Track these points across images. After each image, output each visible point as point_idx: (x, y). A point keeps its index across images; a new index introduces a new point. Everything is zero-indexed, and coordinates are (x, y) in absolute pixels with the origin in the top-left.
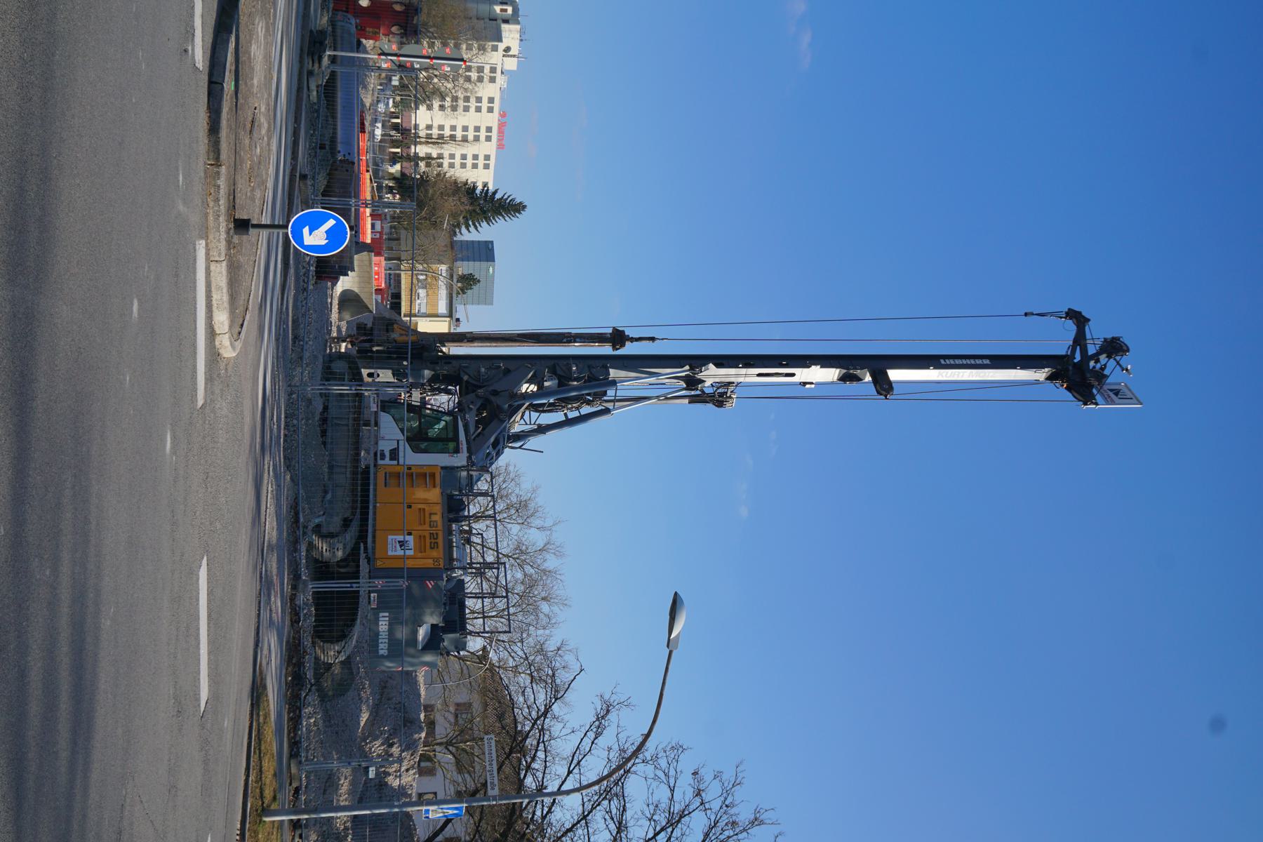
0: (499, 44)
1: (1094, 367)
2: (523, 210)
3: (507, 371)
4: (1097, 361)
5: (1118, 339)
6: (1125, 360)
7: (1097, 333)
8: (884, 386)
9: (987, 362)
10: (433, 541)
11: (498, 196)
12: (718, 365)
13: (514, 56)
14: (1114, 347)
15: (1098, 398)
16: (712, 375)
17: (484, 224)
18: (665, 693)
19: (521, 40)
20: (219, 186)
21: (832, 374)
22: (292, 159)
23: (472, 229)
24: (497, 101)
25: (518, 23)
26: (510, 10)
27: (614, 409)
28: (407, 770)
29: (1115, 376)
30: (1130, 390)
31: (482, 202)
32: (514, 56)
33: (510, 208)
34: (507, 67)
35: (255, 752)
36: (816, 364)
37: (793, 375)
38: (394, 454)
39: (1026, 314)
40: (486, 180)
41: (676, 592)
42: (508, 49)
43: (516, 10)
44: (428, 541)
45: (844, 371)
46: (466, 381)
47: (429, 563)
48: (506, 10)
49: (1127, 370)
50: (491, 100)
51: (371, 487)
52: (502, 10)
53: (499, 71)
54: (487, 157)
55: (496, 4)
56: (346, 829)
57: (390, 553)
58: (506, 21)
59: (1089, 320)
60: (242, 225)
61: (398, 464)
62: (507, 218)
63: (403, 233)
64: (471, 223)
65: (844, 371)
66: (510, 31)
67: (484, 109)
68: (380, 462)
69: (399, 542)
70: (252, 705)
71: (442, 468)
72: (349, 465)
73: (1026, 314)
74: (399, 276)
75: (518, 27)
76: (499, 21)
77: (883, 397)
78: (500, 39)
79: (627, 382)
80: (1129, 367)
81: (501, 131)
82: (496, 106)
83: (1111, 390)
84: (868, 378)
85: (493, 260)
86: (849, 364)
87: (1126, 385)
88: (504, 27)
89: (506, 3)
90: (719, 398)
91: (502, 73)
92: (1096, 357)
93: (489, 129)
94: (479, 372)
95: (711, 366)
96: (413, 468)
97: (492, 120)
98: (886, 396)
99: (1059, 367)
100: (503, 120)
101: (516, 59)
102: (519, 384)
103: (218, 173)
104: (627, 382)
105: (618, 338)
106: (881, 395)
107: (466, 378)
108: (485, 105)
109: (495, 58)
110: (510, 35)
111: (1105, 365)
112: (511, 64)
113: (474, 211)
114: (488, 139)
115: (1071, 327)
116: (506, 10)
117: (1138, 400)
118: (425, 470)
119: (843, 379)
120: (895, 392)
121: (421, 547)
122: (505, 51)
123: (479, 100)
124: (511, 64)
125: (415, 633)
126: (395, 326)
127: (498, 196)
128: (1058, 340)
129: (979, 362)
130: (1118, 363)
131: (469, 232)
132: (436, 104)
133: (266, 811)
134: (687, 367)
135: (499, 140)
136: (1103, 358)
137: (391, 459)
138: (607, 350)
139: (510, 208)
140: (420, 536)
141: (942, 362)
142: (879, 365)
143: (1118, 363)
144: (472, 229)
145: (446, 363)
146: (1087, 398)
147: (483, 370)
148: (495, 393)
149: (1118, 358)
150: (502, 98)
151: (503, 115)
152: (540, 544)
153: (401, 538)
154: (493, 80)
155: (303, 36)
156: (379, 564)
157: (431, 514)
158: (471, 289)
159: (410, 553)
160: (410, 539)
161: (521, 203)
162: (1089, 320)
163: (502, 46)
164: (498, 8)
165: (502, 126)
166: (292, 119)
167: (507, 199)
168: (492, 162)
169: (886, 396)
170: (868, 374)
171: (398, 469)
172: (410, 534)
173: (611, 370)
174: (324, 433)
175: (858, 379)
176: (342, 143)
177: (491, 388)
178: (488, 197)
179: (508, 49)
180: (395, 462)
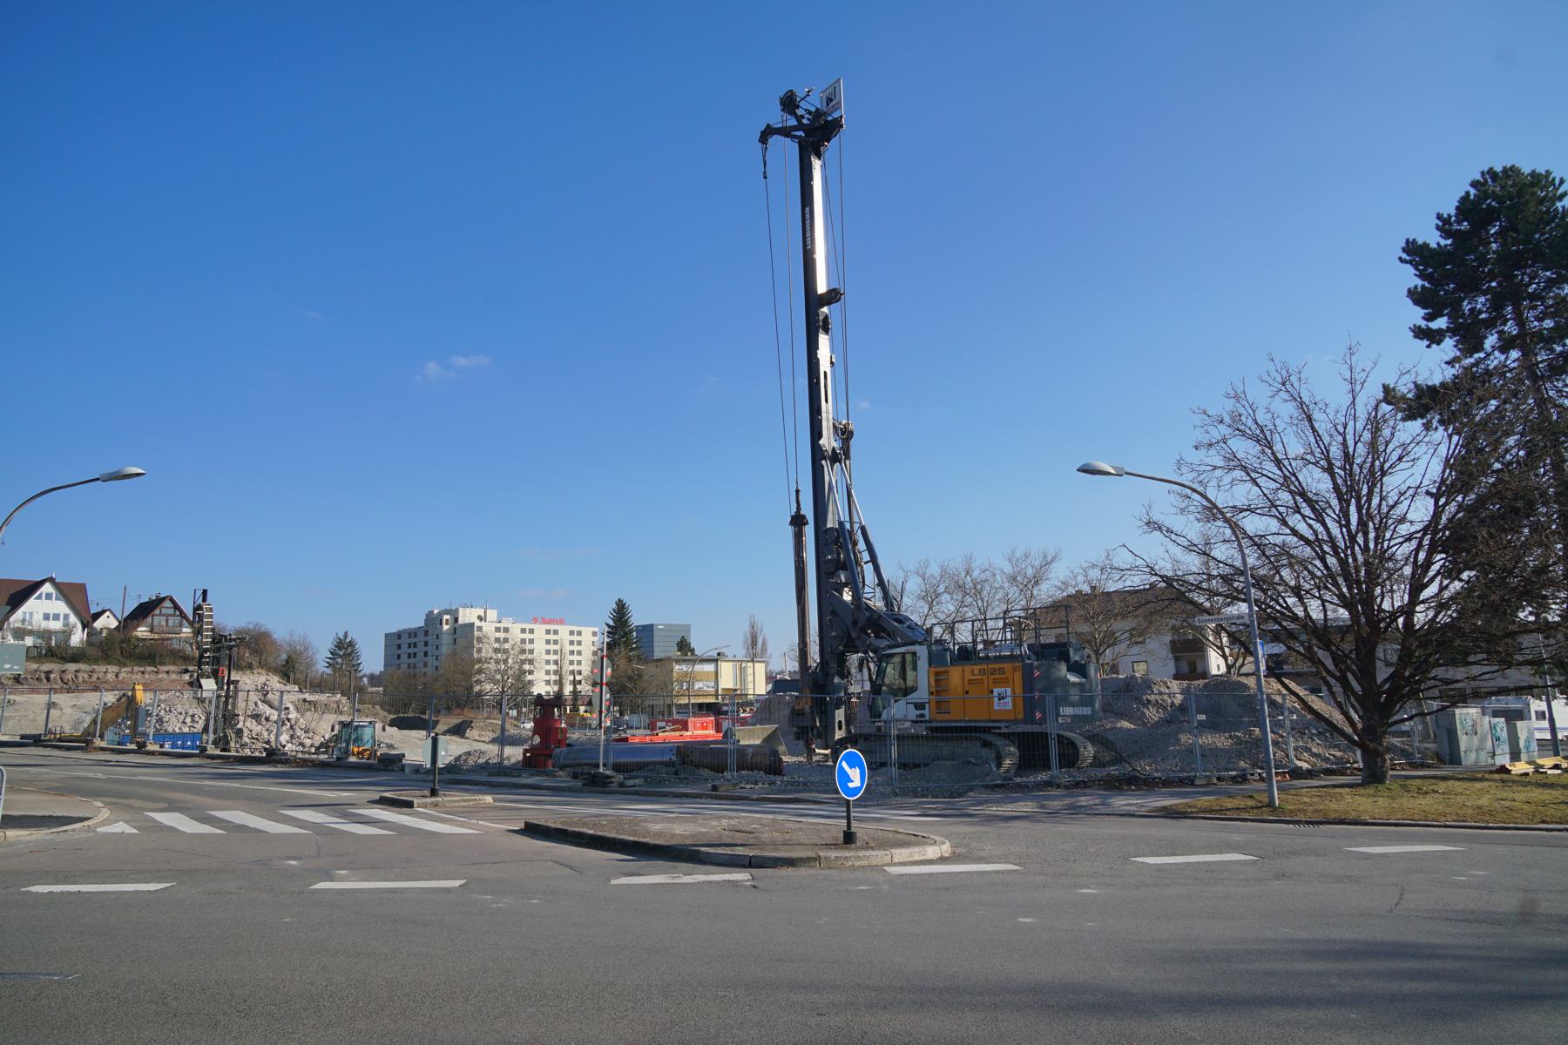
0: (476, 625)
1: (809, 119)
3: (834, 613)
4: (803, 117)
5: (781, 99)
6: (800, 94)
7: (777, 118)
8: (833, 296)
9: (807, 210)
10: (997, 672)
11: (611, 623)
12: (820, 436)
13: (485, 612)
14: (789, 103)
15: (836, 115)
16: (828, 441)
18: (1159, 477)
19: (472, 607)
20: (836, 857)
21: (823, 340)
22: (701, 798)
24: (524, 626)
25: (457, 609)
26: (446, 617)
27: (860, 523)
28: (1168, 688)
29: (814, 102)
30: (827, 89)
31: (617, 637)
32: (485, 612)
33: (621, 611)
34: (495, 619)
35: (1225, 814)
36: (817, 354)
37: (825, 373)
38: (920, 706)
39: (765, 178)
40: (591, 634)
41: (1078, 470)
42: (480, 618)
43: (447, 612)
44: (998, 676)
45: (821, 330)
46: (844, 647)
47: (1018, 676)
48: (447, 620)
49: (809, 92)
50: (523, 631)
51: (953, 724)
52: (447, 624)
54: (572, 633)
55: (442, 629)
56: (1231, 737)
57: (1010, 707)
58: (456, 620)
59: (768, 125)
60: (849, 838)
61: (929, 703)
62: (630, 615)
63: (647, 703)
65: (821, 330)
66: (464, 616)
67: (531, 636)
68: (927, 718)
69: (999, 700)
70: (1185, 818)
71: (930, 666)
72: (935, 744)
73: (765, 178)
74: (693, 704)
75: (461, 609)
77: (843, 297)
79: (837, 514)
80: (807, 90)
81: (549, 622)
82: (528, 626)
83: (828, 105)
84: (825, 309)
85: (653, 625)
86: (815, 326)
87: (823, 92)
88: (461, 621)
89: (441, 620)
90: (845, 434)
91: (500, 622)
92: (799, 118)
93: (548, 632)
94: (835, 637)
95: (821, 442)
96: (932, 690)
97: (540, 629)
98: (841, 294)
99: (810, 149)
100: (540, 620)
102: (844, 602)
103: (826, 858)
104: (837, 514)
105: (798, 521)
106: (840, 298)
107: (841, 648)
108: (527, 636)
109: (488, 628)
110: (467, 616)
111: (806, 110)
112: (492, 614)
113: (624, 642)
114: (556, 632)
115: (774, 140)
117: (836, 82)
118: (932, 680)
119: (827, 331)
120: (837, 287)
121: (1004, 682)
122: (481, 620)
123: (523, 641)
124: (492, 614)
125: (1074, 684)
126: (797, 708)
127: (611, 623)
128: (785, 150)
129: (808, 216)
130: (803, 99)
132: (529, 677)
133: (1271, 804)
134: (823, 462)
136: (800, 112)
137: (923, 708)
138: (809, 531)
139: (621, 611)
140: (994, 683)
141: (809, 247)
142: (814, 302)
143: (803, 99)
145: (827, 665)
146: (836, 125)
147: (833, 634)
148: (855, 623)
149: (798, 99)
150: (522, 622)
151: (535, 621)
152: (919, 580)
153: (996, 699)
154: (506, 630)
155: (589, 792)
156: (1020, 716)
157: (973, 674)
159: (1009, 690)
160: (996, 691)
161: (617, 603)
162: (768, 125)
163: (478, 623)
164: (446, 627)
165: (545, 622)
166: (666, 799)
168: (576, 629)
169: (841, 294)
170: (822, 310)
171: (933, 704)
172: (992, 692)
173: (828, 526)
174: (917, 766)
175: (826, 317)
176: (663, 757)
177: (851, 627)
178: (612, 631)
179: (480, 618)
180: (927, 705)
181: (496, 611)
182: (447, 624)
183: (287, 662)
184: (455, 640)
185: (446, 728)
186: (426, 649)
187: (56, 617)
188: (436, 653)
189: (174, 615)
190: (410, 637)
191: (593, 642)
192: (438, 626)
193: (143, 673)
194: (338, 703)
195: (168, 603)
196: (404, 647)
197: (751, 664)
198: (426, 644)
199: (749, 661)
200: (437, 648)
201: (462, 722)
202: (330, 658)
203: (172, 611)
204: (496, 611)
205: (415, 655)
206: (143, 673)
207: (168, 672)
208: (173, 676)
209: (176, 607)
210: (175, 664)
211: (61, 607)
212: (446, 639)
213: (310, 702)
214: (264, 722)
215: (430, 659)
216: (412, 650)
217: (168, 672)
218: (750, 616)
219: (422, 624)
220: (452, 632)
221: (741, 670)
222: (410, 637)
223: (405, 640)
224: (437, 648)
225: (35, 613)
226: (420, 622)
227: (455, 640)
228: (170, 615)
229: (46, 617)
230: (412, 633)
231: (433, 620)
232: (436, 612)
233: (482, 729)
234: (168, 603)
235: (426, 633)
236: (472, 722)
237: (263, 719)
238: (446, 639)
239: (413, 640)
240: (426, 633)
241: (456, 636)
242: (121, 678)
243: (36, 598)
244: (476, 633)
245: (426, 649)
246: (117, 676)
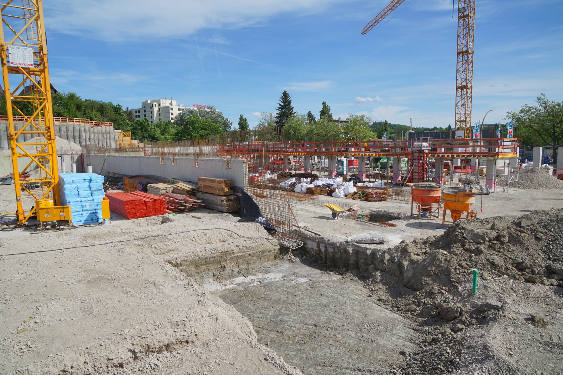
19: (166, 99)
25: (160, 100)
33: (285, 97)
58: (159, 105)
75: (161, 100)
76: (160, 107)
78: (168, 107)
88: (162, 105)
89: (153, 105)
110: (165, 103)
112: (174, 103)
163: (171, 107)
178: (282, 108)
181: (176, 101)
184: (160, 114)
190: (136, 112)
204: (176, 101)
226: (139, 106)
227: (160, 114)
232: (149, 102)
235: (145, 111)
240: (145, 111)
241: (160, 112)
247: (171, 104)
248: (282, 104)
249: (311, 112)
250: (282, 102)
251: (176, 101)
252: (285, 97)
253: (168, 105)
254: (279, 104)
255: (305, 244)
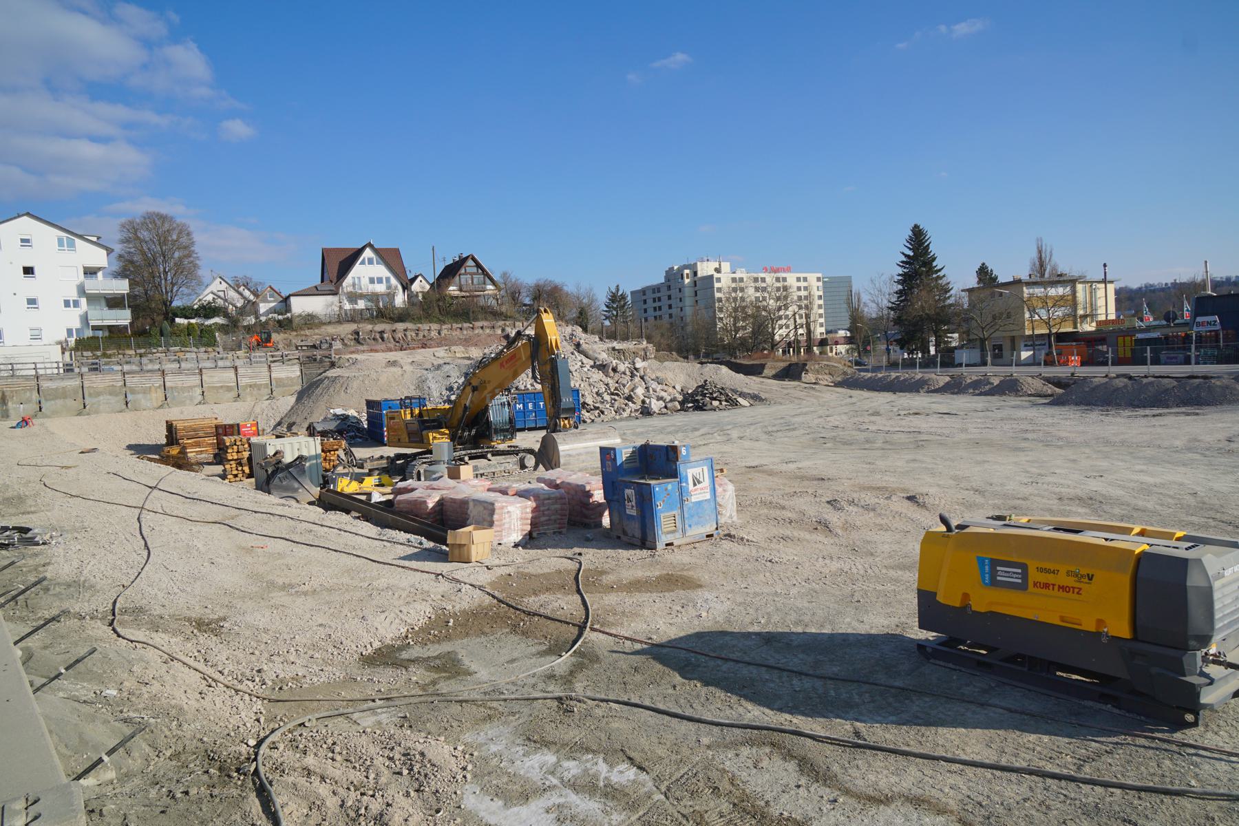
2: (919, 227)
13: (720, 265)
17: (934, 264)
19: (708, 260)
23: (941, 274)
24: (755, 275)
25: (696, 264)
26: (687, 271)
32: (720, 265)
33: (918, 238)
40: (815, 279)
43: (686, 267)
48: (687, 274)
52: (688, 278)
53: (734, 276)
54: (798, 279)
55: (684, 282)
58: (695, 274)
64: (934, 276)
75: (699, 264)
76: (696, 278)
88: (700, 274)
89: (682, 275)
91: (734, 273)
101: (722, 263)
110: (705, 269)
112: (726, 267)
116: (687, 274)
131: (944, 276)
135: (784, 271)
144: (941, 274)
151: (766, 270)
154: (741, 280)
158: (991, 271)
164: (687, 281)
167: (910, 244)
178: (909, 261)
181: (728, 264)
182: (688, 278)
183: (581, 313)
184: (696, 292)
185: (774, 372)
186: (670, 302)
187: (380, 280)
188: (680, 305)
189: (477, 273)
190: (654, 292)
191: (818, 287)
192: (680, 280)
193: (461, 329)
194: (645, 350)
195: (470, 262)
196: (650, 302)
197: (1103, 285)
198: (669, 297)
199: (1099, 282)
200: (681, 301)
201: (790, 365)
202: (606, 311)
203: (475, 270)
204: (728, 264)
205: (660, 308)
206: (461, 329)
207: (482, 328)
208: (488, 331)
209: (478, 265)
210: (486, 319)
211: (381, 271)
212: (688, 292)
213: (619, 351)
214: (612, 374)
215: (673, 311)
216: (657, 304)
217: (482, 328)
218: (1037, 240)
219: (663, 280)
220: (693, 285)
221: (1091, 293)
222: (654, 292)
223: (650, 296)
224: (681, 301)
225: (362, 278)
226: (659, 279)
227: (696, 292)
228: (475, 274)
229: (372, 281)
230: (656, 289)
231: (673, 277)
232: (676, 268)
233: (818, 372)
234: (470, 262)
235: (669, 288)
236: (806, 365)
237: (610, 370)
238: (688, 292)
239: (657, 295)
240: (669, 288)
241: (697, 288)
242: (443, 335)
243: (361, 263)
244: (717, 285)
245: (670, 302)
246: (439, 333)
247: (718, 270)
248: (911, 254)
249: (987, 264)
250: (910, 249)
251: (728, 264)
252: (918, 238)
253: (711, 271)
254: (903, 254)
255: (36, 372)
